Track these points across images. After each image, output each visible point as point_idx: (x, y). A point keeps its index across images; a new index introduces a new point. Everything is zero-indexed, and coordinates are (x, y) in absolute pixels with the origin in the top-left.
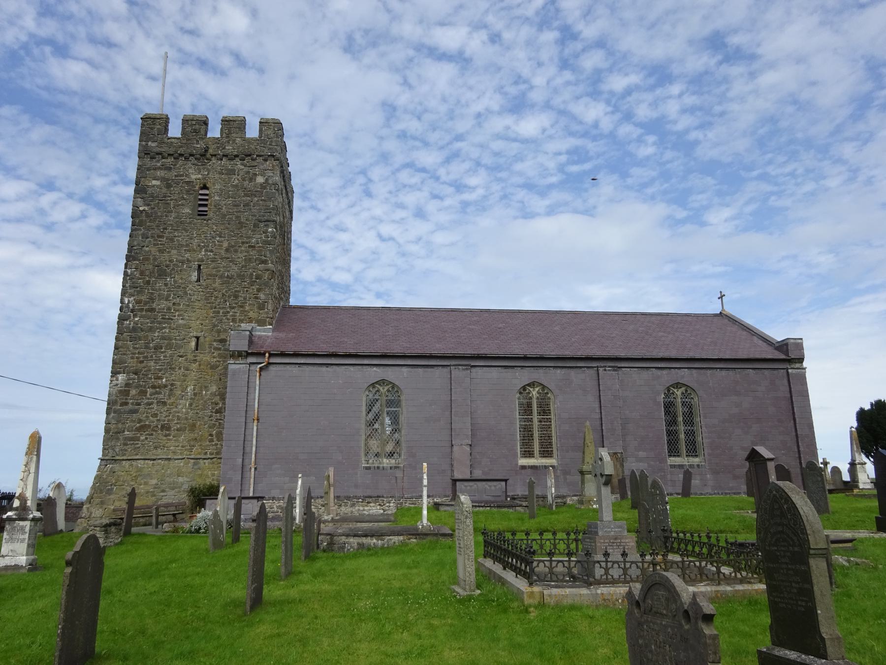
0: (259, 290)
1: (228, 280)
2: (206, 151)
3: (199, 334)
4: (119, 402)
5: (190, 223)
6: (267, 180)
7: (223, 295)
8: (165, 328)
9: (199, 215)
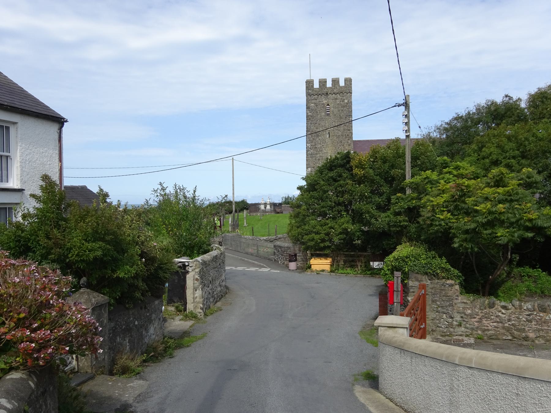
1: (338, 137)
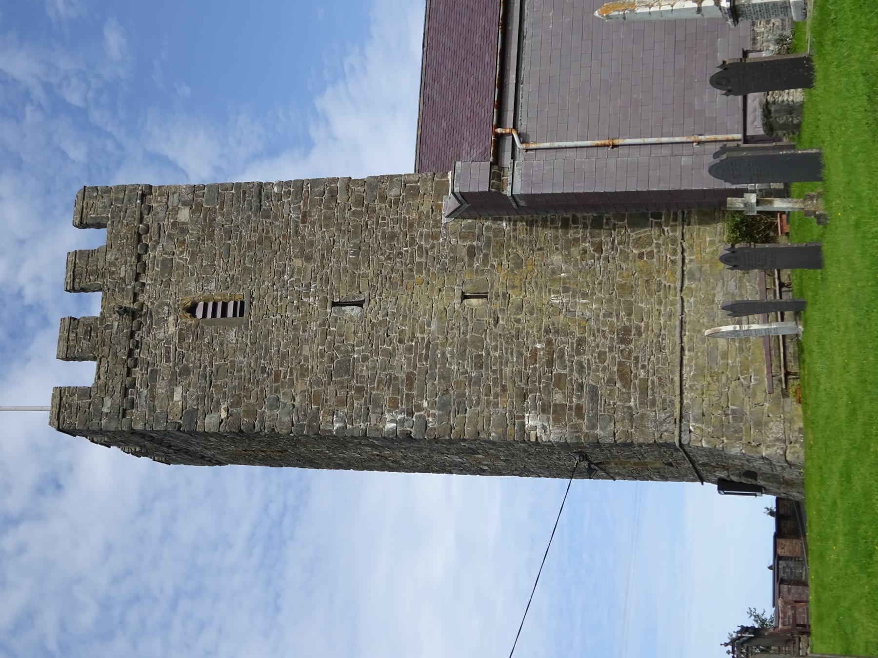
0: (383, 199)
2: (126, 310)
3: (458, 294)
4: (576, 421)
5: (255, 328)
6: (185, 204)
7: (389, 258)
8: (443, 354)
9: (241, 315)
